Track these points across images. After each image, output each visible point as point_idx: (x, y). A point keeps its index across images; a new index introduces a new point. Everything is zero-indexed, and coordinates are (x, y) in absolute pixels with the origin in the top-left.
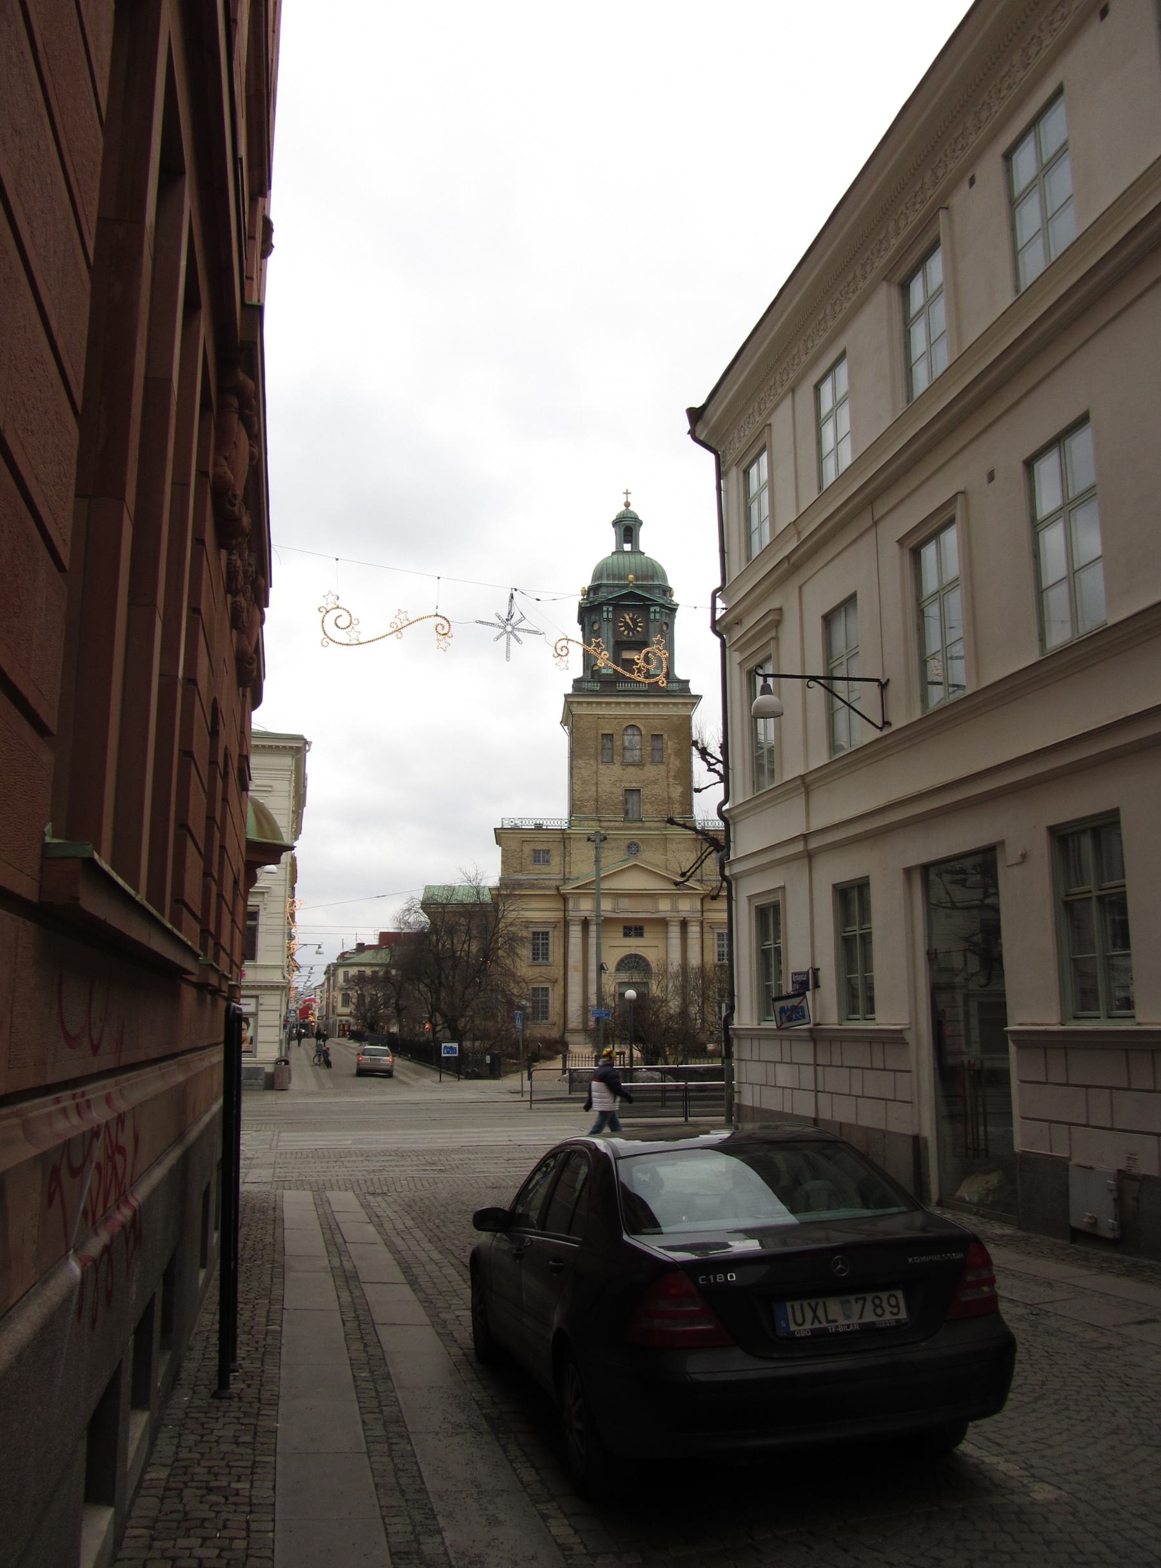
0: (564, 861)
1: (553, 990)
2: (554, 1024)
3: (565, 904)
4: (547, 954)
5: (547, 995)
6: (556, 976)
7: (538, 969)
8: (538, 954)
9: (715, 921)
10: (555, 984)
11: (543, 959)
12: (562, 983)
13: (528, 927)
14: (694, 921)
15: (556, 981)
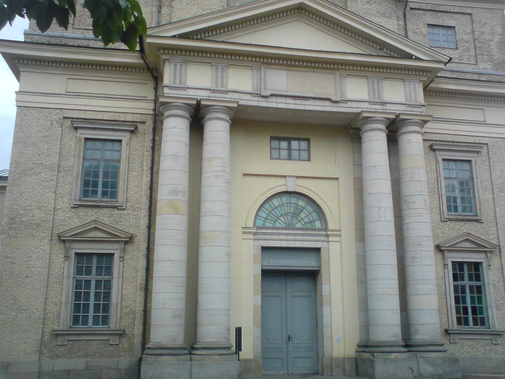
0: (159, 12)
1: (122, 258)
2: (121, 334)
3: (156, 89)
4: (115, 186)
5: (109, 270)
6: (131, 231)
7: (91, 215)
8: (95, 184)
9: (438, 137)
10: (129, 248)
11: (104, 194)
12: (143, 246)
13: (76, 128)
14: (415, 123)
15: (130, 240)
